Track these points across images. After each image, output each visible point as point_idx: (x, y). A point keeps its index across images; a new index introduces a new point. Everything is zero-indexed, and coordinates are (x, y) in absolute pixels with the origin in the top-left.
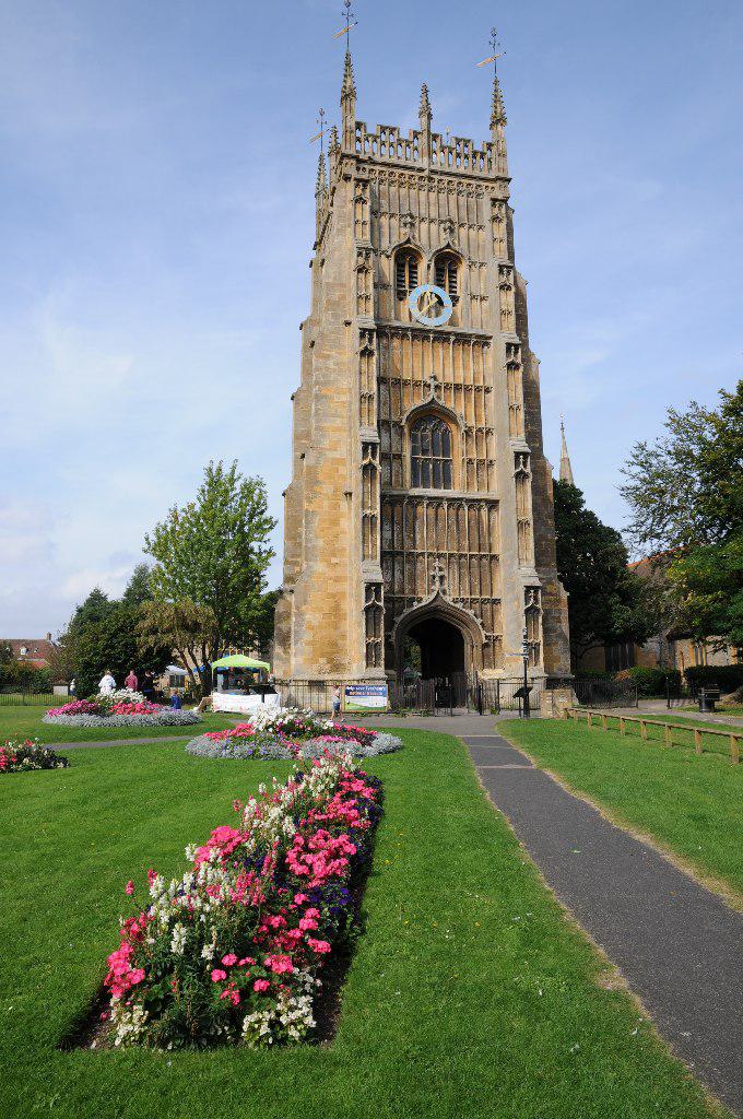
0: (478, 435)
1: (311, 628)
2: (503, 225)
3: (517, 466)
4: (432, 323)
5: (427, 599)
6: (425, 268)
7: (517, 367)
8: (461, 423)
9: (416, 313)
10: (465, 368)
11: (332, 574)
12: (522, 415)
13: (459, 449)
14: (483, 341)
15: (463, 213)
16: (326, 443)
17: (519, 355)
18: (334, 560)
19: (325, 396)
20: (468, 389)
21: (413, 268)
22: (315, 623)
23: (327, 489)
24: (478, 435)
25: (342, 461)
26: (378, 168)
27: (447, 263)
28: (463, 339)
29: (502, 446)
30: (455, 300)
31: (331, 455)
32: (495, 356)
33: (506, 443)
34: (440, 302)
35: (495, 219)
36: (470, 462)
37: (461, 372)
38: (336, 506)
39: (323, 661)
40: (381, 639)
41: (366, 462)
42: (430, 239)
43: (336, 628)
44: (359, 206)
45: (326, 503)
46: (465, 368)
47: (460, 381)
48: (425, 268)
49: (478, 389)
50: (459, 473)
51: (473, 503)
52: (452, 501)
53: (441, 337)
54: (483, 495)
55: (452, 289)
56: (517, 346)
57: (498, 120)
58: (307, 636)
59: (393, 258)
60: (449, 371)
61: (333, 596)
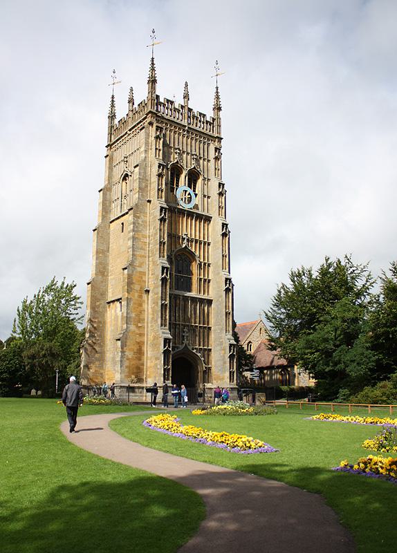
1: (128, 359)
4: (187, 207)
5: (182, 347)
6: (183, 178)
8: (197, 259)
11: (137, 331)
18: (139, 325)
22: (130, 357)
23: (137, 287)
27: (193, 177)
31: (139, 269)
36: (200, 279)
38: (140, 297)
39: (133, 376)
42: (188, 164)
43: (140, 359)
45: (136, 295)
49: (205, 243)
51: (202, 301)
52: (194, 300)
54: (205, 297)
55: (194, 191)
57: (218, 108)
58: (126, 363)
61: (139, 343)
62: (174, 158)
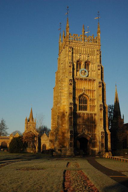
0: (93, 100)
2: (99, 56)
3: (100, 107)
5: (82, 133)
6: (83, 63)
7: (101, 86)
9: (81, 75)
10: (90, 86)
12: (101, 97)
13: (89, 103)
14: (94, 80)
15: (91, 53)
16: (62, 102)
17: (102, 86)
19: (62, 92)
20: (91, 91)
21: (80, 64)
24: (93, 100)
25: (65, 105)
26: (73, 43)
27: (87, 64)
28: (90, 80)
29: (97, 103)
30: (89, 71)
31: (63, 104)
32: (96, 85)
33: (98, 103)
34: (85, 72)
35: (97, 54)
36: (91, 106)
37: (89, 87)
40: (73, 142)
41: (70, 106)
44: (69, 52)
46: (90, 86)
47: (89, 89)
48: (83, 63)
49: (93, 90)
50: (88, 108)
53: (86, 80)
56: (101, 82)
59: (76, 63)
60: (87, 87)
62: (77, 57)
